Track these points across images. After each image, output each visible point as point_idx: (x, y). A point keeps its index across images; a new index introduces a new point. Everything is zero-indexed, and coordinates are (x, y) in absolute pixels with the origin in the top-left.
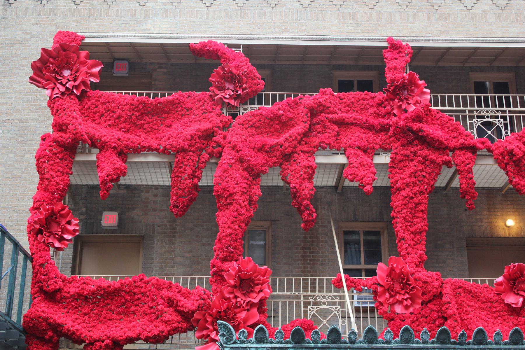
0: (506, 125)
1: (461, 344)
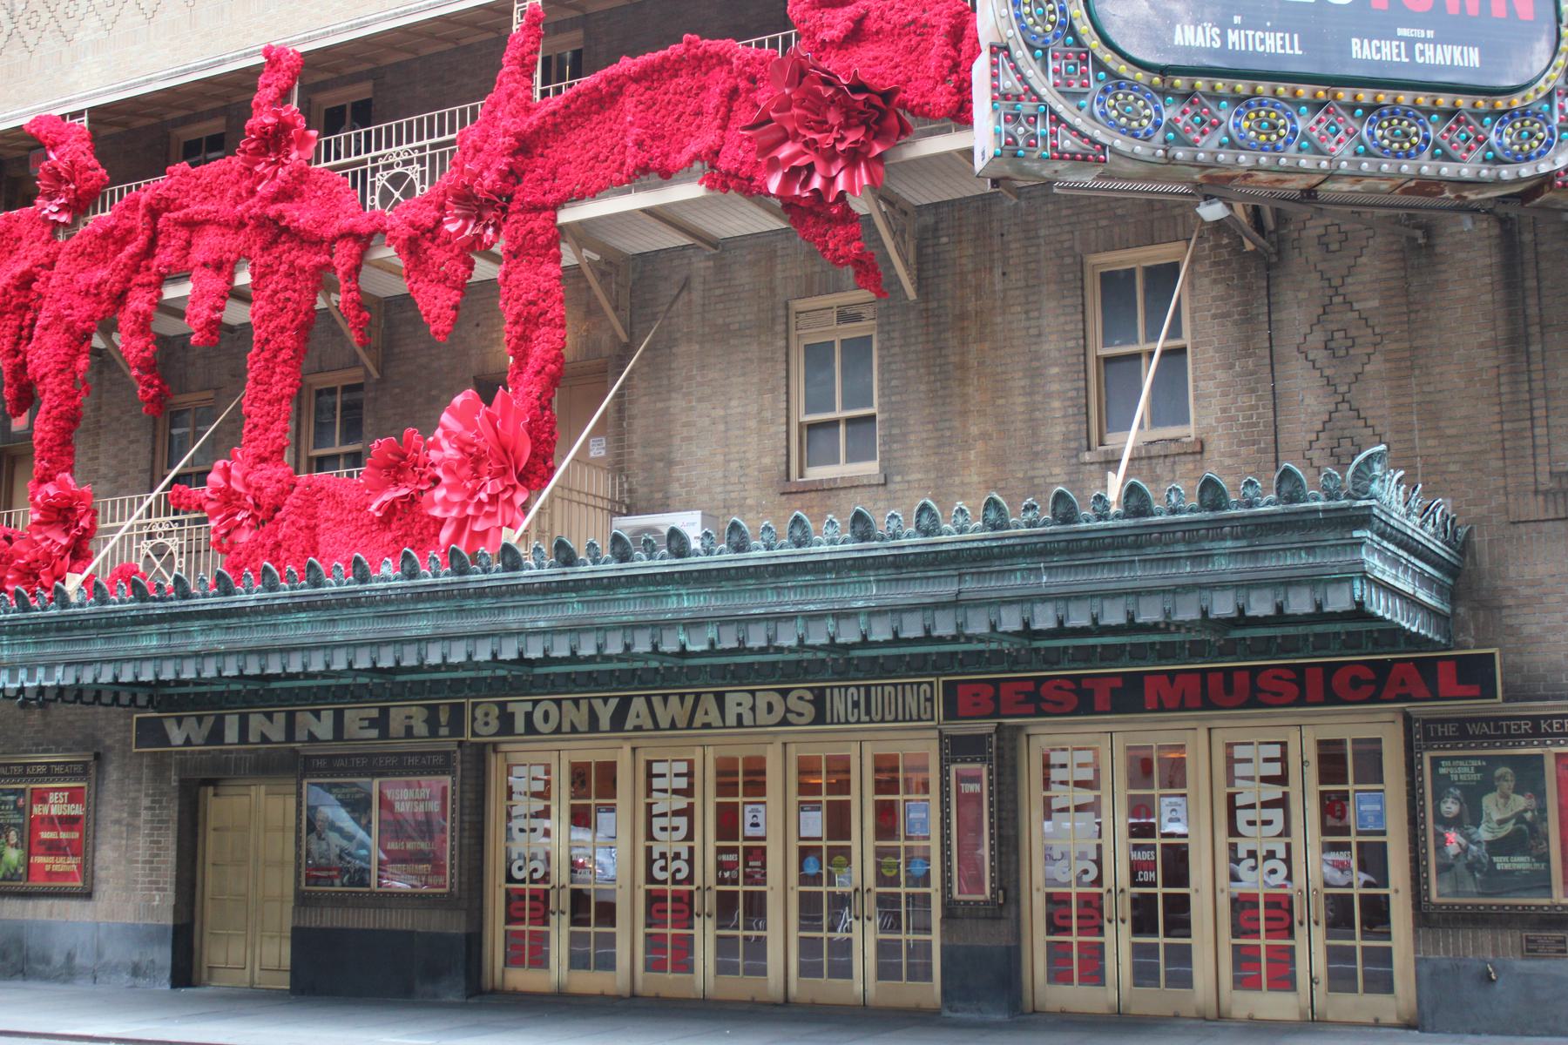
0: (423, 173)
1: (161, 600)
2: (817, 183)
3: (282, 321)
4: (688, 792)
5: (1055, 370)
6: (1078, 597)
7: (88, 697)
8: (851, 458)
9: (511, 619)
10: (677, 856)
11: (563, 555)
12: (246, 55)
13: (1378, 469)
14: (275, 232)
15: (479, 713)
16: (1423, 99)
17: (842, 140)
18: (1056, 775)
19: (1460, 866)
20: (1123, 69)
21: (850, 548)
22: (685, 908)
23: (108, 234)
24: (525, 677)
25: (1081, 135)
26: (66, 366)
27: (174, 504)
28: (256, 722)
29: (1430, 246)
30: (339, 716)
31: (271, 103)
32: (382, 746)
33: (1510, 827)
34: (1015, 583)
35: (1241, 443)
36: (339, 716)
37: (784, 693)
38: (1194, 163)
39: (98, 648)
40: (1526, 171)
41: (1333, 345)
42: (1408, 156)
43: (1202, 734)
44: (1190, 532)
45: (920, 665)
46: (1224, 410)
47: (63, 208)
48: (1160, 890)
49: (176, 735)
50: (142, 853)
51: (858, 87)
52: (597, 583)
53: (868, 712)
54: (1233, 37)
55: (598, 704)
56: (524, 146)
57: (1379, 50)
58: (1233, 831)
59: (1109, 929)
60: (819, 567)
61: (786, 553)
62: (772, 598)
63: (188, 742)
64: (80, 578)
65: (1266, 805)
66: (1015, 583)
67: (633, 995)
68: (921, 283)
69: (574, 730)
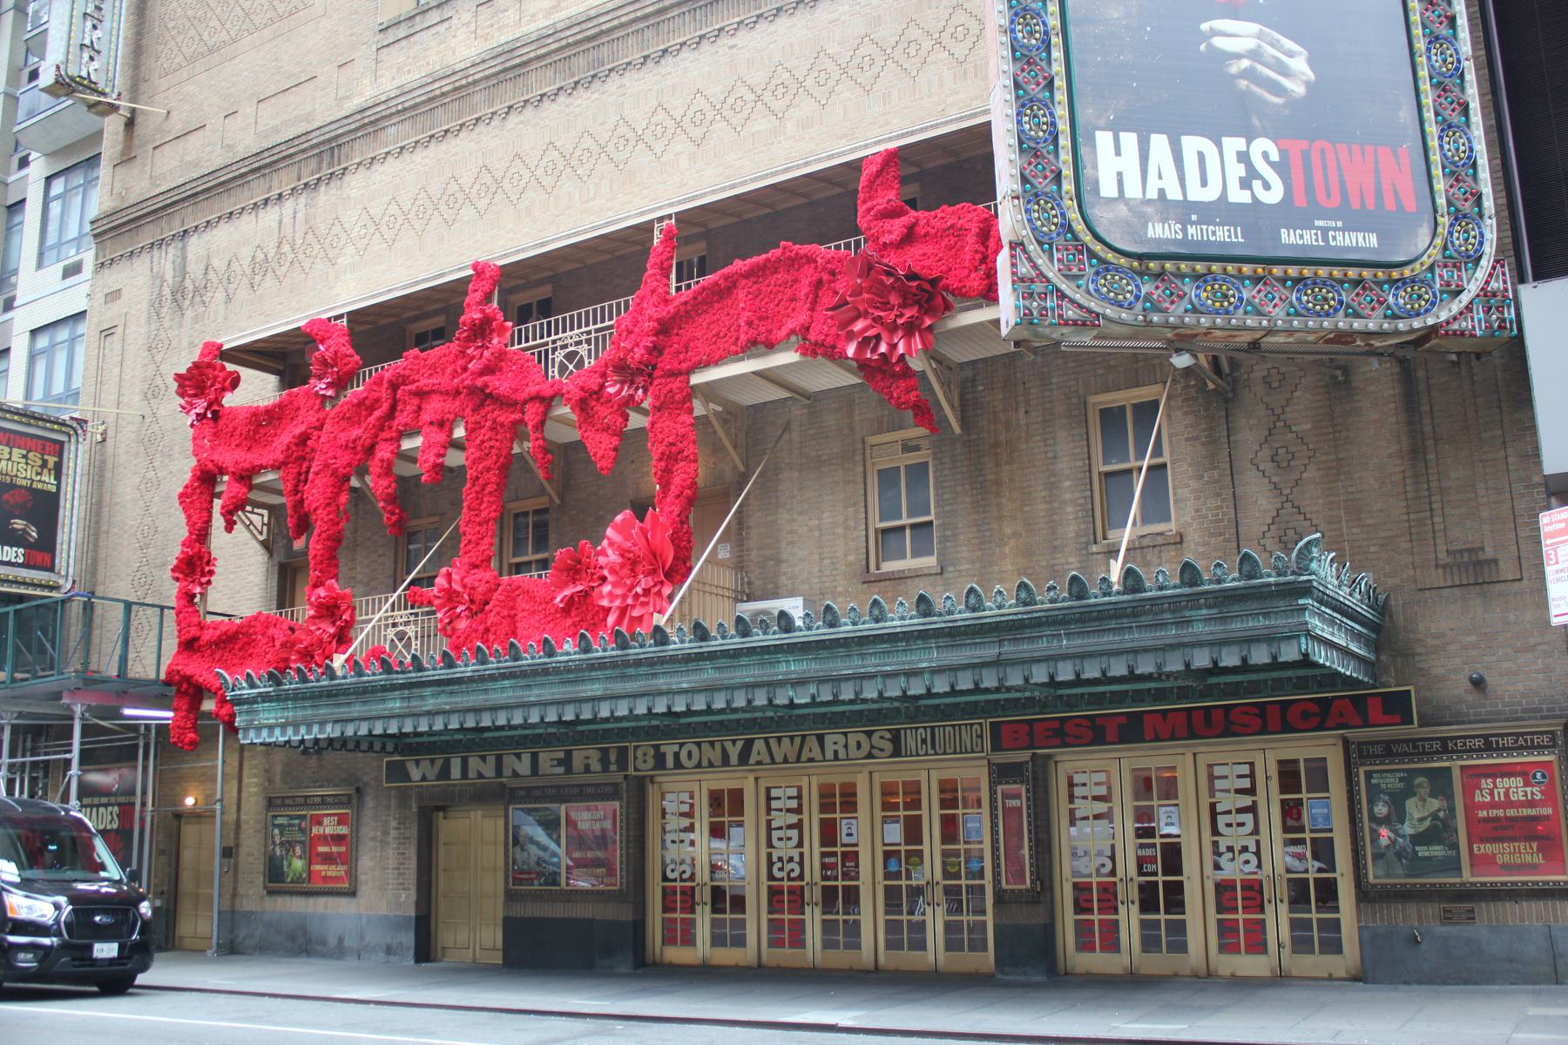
1: (403, 672)
2: (883, 348)
3: (487, 463)
4: (798, 811)
5: (1067, 484)
6: (1091, 655)
7: (351, 746)
8: (915, 554)
9: (662, 682)
10: (791, 860)
11: (699, 633)
12: (460, 269)
13: (1315, 552)
14: (482, 398)
15: (639, 753)
16: (1337, 272)
17: (901, 315)
18: (1078, 791)
19: (1390, 854)
20: (1110, 256)
21: (916, 623)
22: (798, 899)
23: (361, 403)
24: (673, 725)
25: (1080, 306)
26: (332, 500)
27: (412, 601)
28: (474, 763)
29: (1347, 382)
30: (535, 757)
31: (478, 303)
32: (567, 780)
33: (1427, 823)
34: (1043, 646)
35: (1211, 535)
36: (535, 757)
37: (869, 734)
38: (1167, 325)
39: (357, 709)
40: (1416, 324)
41: (1277, 458)
42: (1327, 315)
43: (1189, 757)
44: (1175, 604)
45: (971, 710)
46: (1197, 511)
47: (329, 386)
48: (1160, 878)
49: (415, 774)
50: (392, 863)
51: (912, 276)
52: (725, 654)
53: (933, 747)
54: (1191, 230)
55: (728, 745)
56: (664, 328)
57: (1301, 237)
58: (1215, 831)
59: (1122, 909)
60: (892, 638)
61: (868, 627)
62: (857, 662)
63: (424, 779)
64: (343, 657)
65: (1239, 811)
66: (1043, 646)
67: (760, 966)
68: (964, 420)
69: (711, 765)
